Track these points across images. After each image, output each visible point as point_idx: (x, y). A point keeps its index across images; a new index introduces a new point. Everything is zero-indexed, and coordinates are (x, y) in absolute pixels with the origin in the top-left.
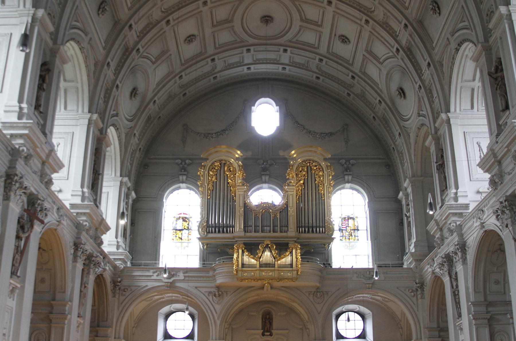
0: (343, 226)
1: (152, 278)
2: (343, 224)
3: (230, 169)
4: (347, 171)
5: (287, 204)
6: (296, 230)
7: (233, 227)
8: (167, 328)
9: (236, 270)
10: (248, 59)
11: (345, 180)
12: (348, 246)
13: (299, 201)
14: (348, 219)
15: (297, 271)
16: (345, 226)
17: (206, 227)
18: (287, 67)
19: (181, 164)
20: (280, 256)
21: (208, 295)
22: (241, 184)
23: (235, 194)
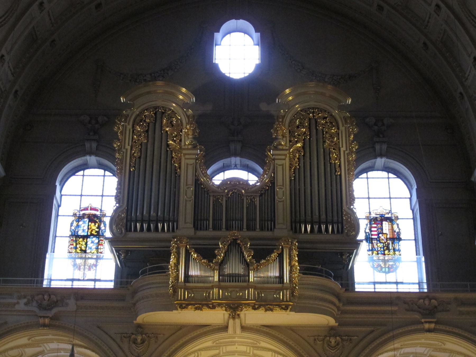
1: (17, 307)
2: (373, 229)
4: (379, 137)
5: (273, 182)
6: (289, 228)
9: (172, 286)
11: (375, 150)
12: (382, 268)
13: (295, 177)
14: (382, 221)
16: (376, 233)
17: (125, 221)
19: (90, 122)
20: (258, 261)
22: (190, 147)
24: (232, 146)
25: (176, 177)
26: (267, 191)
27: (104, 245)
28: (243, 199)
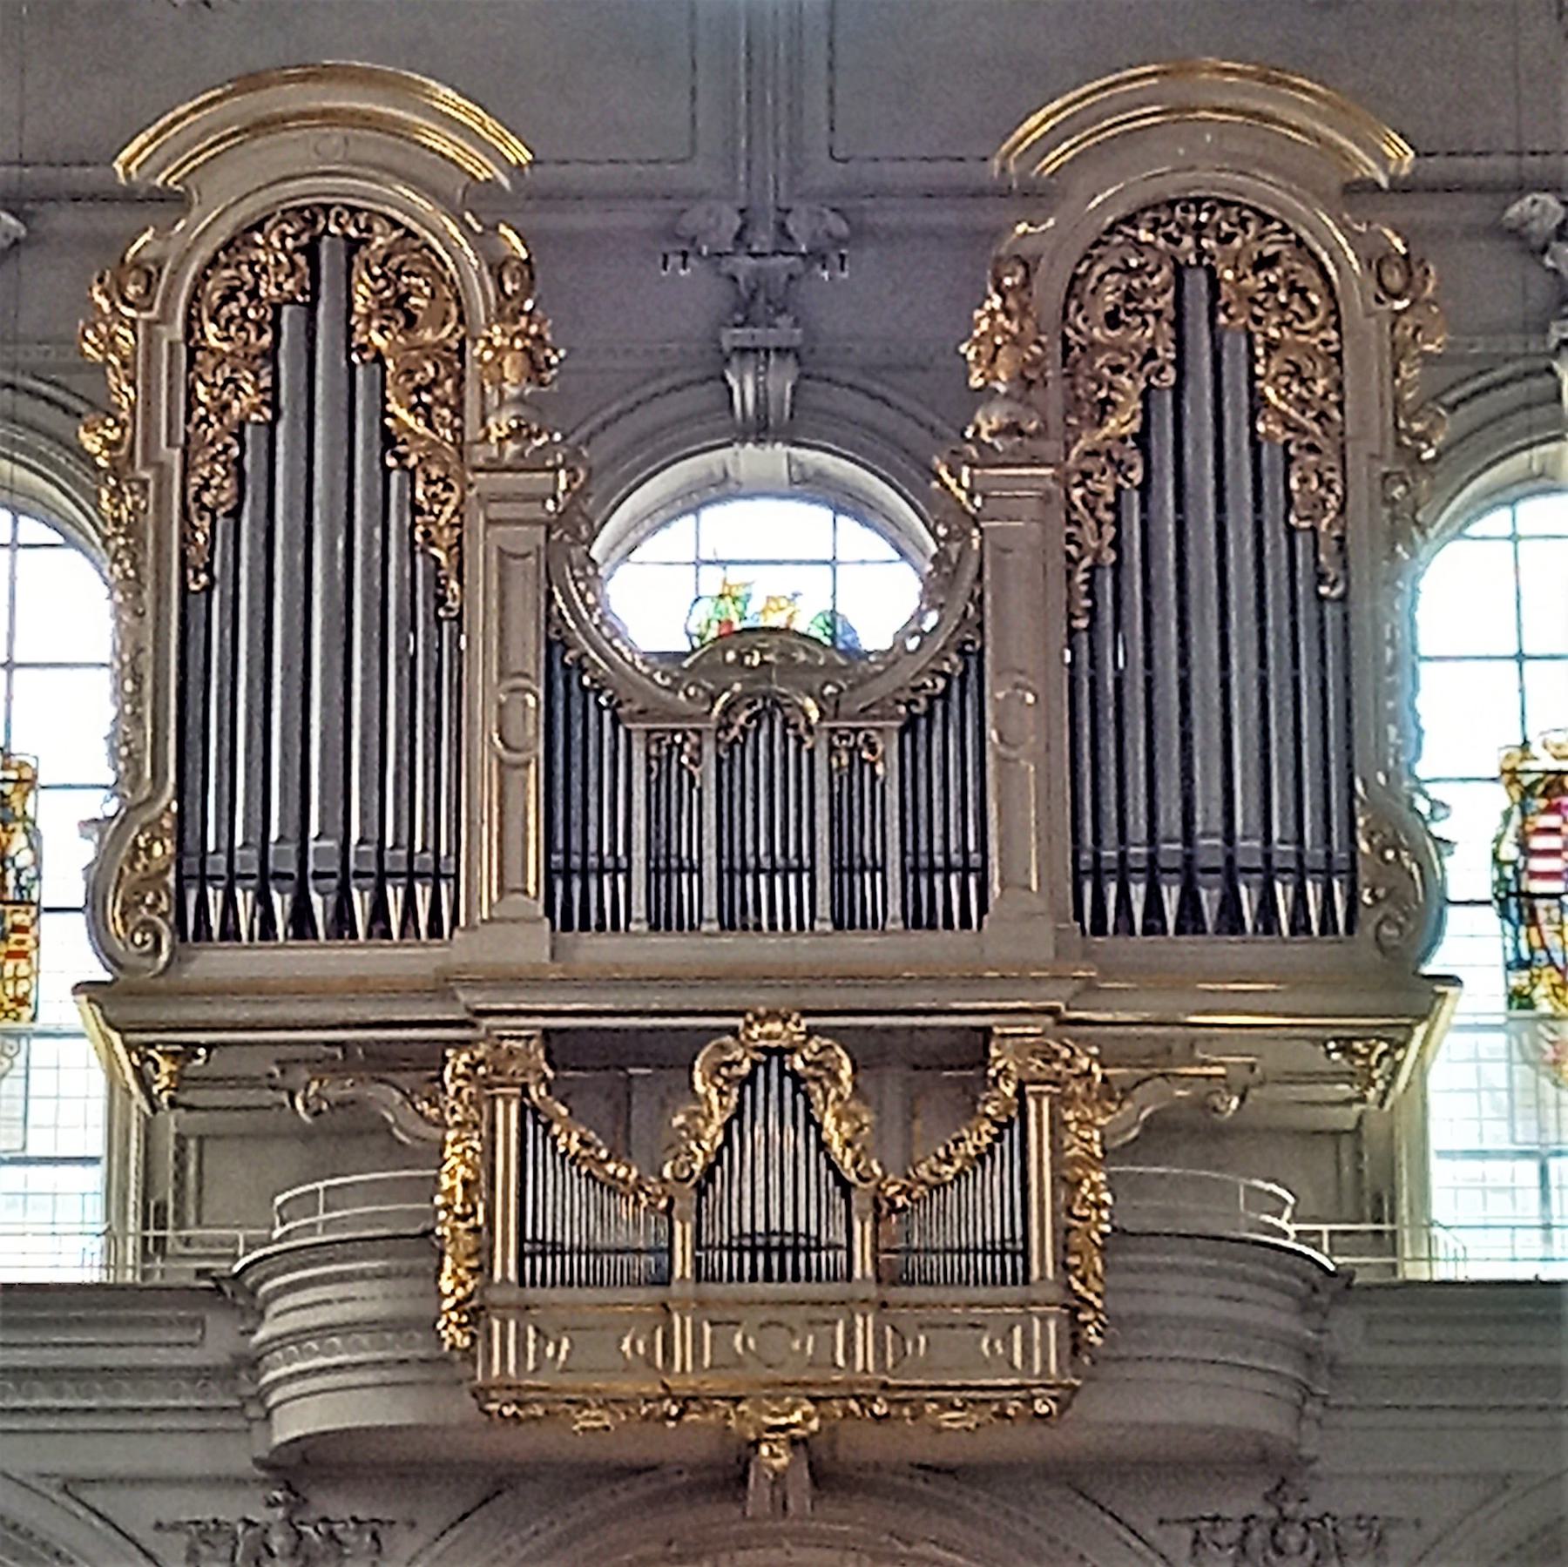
0: (1537, 864)
2: (1538, 843)
3: (401, 299)
17: (171, 878)
25: (439, 621)
26: (939, 705)
27: (33, 954)
28: (811, 752)
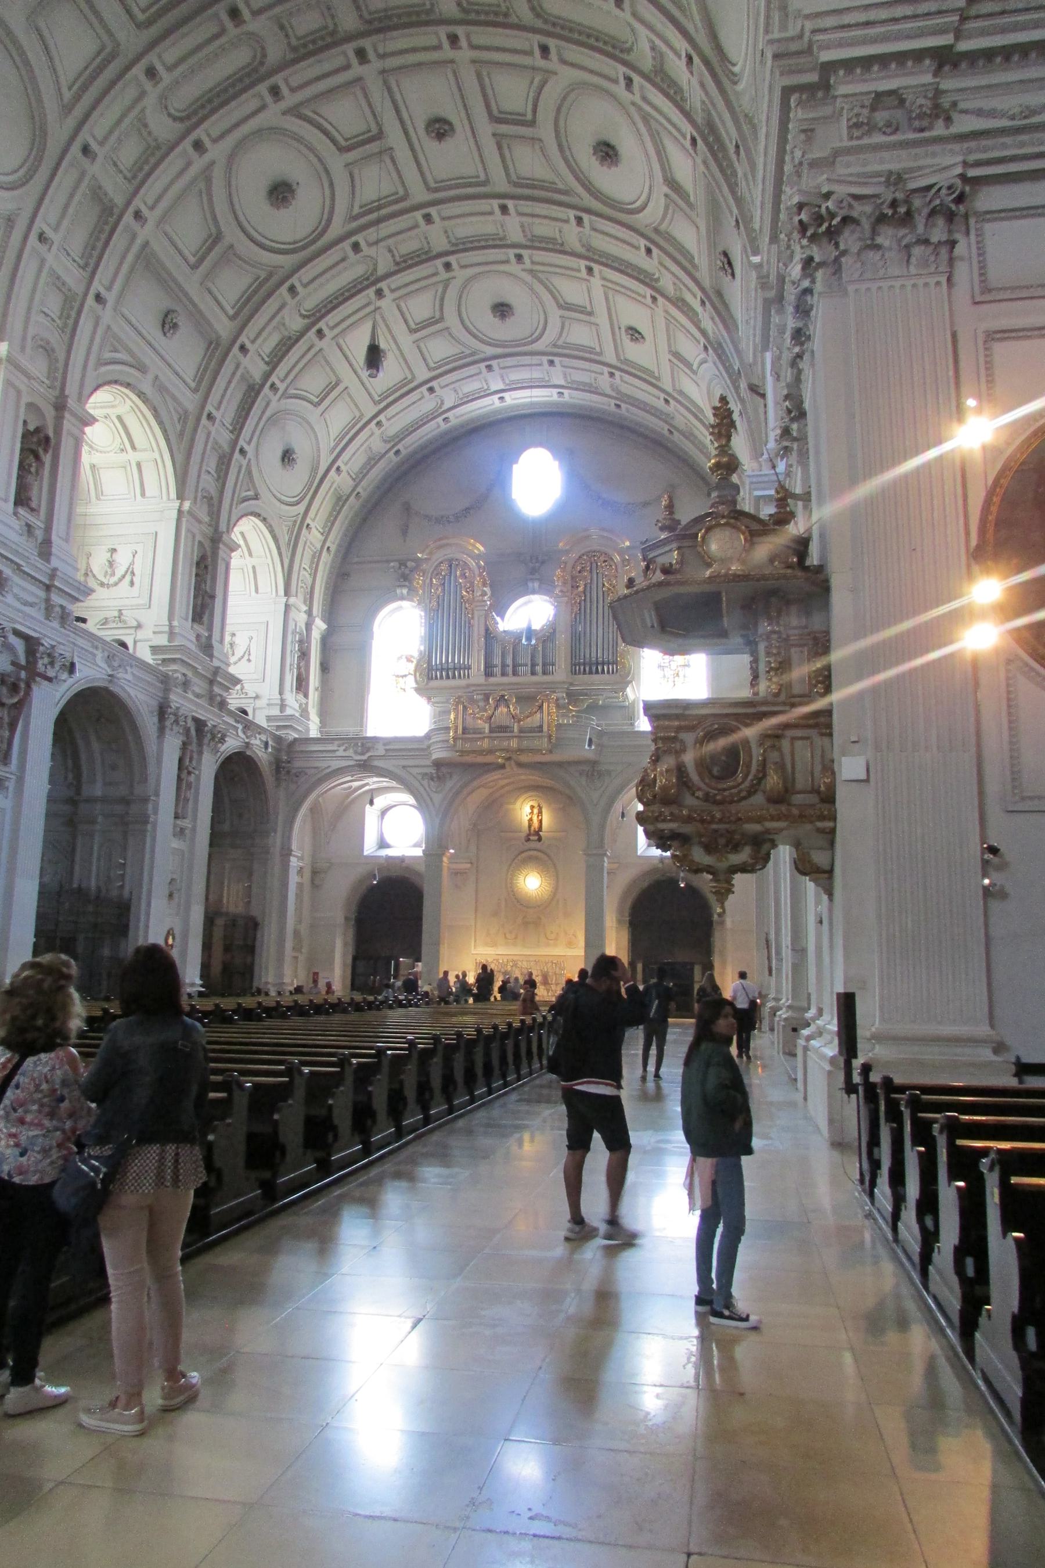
1: (338, 754)
7: (469, 668)
8: (384, 831)
10: (496, 385)
15: (550, 737)
18: (566, 392)
21: (423, 779)
23: (473, 614)
24: (530, 584)
